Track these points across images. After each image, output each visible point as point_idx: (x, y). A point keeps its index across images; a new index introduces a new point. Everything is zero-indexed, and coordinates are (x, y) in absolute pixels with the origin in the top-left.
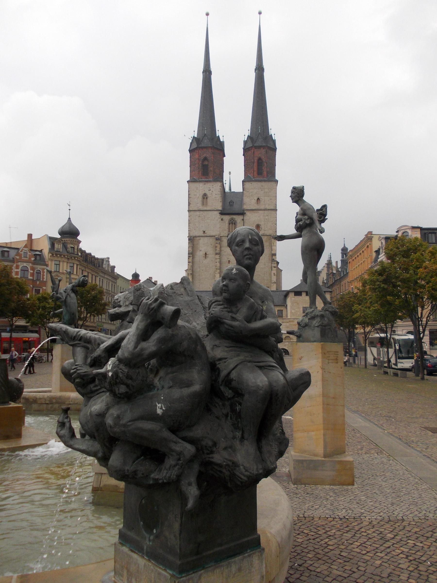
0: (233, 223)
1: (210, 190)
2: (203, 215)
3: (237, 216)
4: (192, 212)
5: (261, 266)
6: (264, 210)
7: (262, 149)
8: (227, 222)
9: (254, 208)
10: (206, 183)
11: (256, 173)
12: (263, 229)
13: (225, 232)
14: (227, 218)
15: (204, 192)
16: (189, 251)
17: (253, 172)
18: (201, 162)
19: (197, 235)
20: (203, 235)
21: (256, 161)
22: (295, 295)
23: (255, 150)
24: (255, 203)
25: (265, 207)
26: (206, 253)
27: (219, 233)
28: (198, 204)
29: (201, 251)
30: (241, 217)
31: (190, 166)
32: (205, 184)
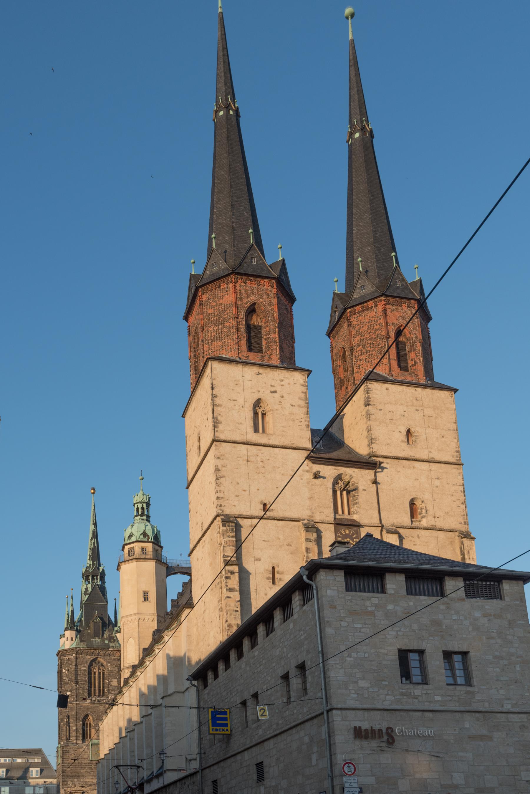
1: (275, 392)
2: (259, 459)
3: (356, 470)
4: (224, 444)
6: (429, 462)
8: (330, 485)
10: (261, 371)
12: (431, 512)
15: (256, 397)
16: (224, 556)
18: (242, 316)
19: (245, 513)
21: (392, 334)
24: (403, 441)
25: (431, 456)
30: (367, 475)
32: (259, 374)
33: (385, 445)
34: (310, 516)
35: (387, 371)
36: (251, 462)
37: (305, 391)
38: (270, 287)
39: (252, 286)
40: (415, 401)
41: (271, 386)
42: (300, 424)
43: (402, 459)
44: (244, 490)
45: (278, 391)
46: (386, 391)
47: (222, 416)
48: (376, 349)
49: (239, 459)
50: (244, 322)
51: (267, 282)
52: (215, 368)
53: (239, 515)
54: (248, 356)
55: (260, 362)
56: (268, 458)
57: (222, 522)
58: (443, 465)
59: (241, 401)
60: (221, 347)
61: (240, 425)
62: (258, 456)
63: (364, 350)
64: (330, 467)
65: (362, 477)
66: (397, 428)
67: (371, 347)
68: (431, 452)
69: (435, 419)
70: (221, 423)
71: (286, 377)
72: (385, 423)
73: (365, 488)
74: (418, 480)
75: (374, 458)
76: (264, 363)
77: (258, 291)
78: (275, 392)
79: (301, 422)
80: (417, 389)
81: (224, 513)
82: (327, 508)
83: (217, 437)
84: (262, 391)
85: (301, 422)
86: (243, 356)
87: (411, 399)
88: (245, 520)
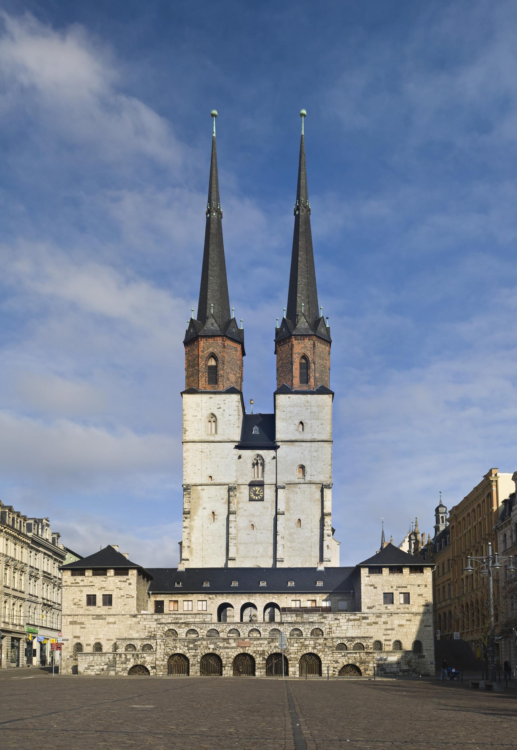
0: (259, 462)
1: (220, 408)
2: (208, 450)
3: (265, 451)
5: (306, 535)
6: (311, 442)
7: (306, 340)
9: (293, 439)
10: (212, 396)
11: (296, 381)
13: (245, 478)
14: (249, 455)
17: (291, 379)
20: (209, 481)
22: (370, 573)
23: (295, 342)
25: (313, 437)
26: (213, 513)
27: (235, 479)
28: (199, 432)
29: (204, 508)
30: (272, 453)
31: (186, 369)
32: (210, 398)
33: (285, 434)
34: (235, 481)
35: (291, 385)
36: (204, 452)
37: (238, 405)
38: (221, 341)
39: (210, 341)
40: (306, 404)
41: (218, 404)
42: (234, 426)
43: (293, 442)
44: (199, 469)
45: (221, 408)
46: (288, 399)
47: (188, 427)
48: (288, 370)
49: (197, 451)
50: (204, 366)
51: (218, 338)
52: (186, 398)
53: (195, 484)
54: (205, 387)
55: (212, 390)
56: (213, 449)
57: (184, 489)
58: (319, 442)
59: (199, 417)
60: (193, 381)
61: (198, 431)
62: (208, 448)
63: (283, 370)
64: (249, 451)
65: (269, 455)
66: (293, 422)
67: (286, 369)
68: (313, 435)
69: (318, 413)
70: (188, 431)
71: (227, 397)
72: (286, 419)
73: (270, 462)
74: (302, 453)
75: (278, 443)
76: (214, 391)
77: (214, 344)
78: (220, 408)
79: (234, 425)
80: (308, 395)
81: (187, 483)
82: (246, 475)
83: (185, 440)
84: (212, 408)
85: (234, 425)
86: (202, 387)
87: (304, 402)
88: (198, 486)
